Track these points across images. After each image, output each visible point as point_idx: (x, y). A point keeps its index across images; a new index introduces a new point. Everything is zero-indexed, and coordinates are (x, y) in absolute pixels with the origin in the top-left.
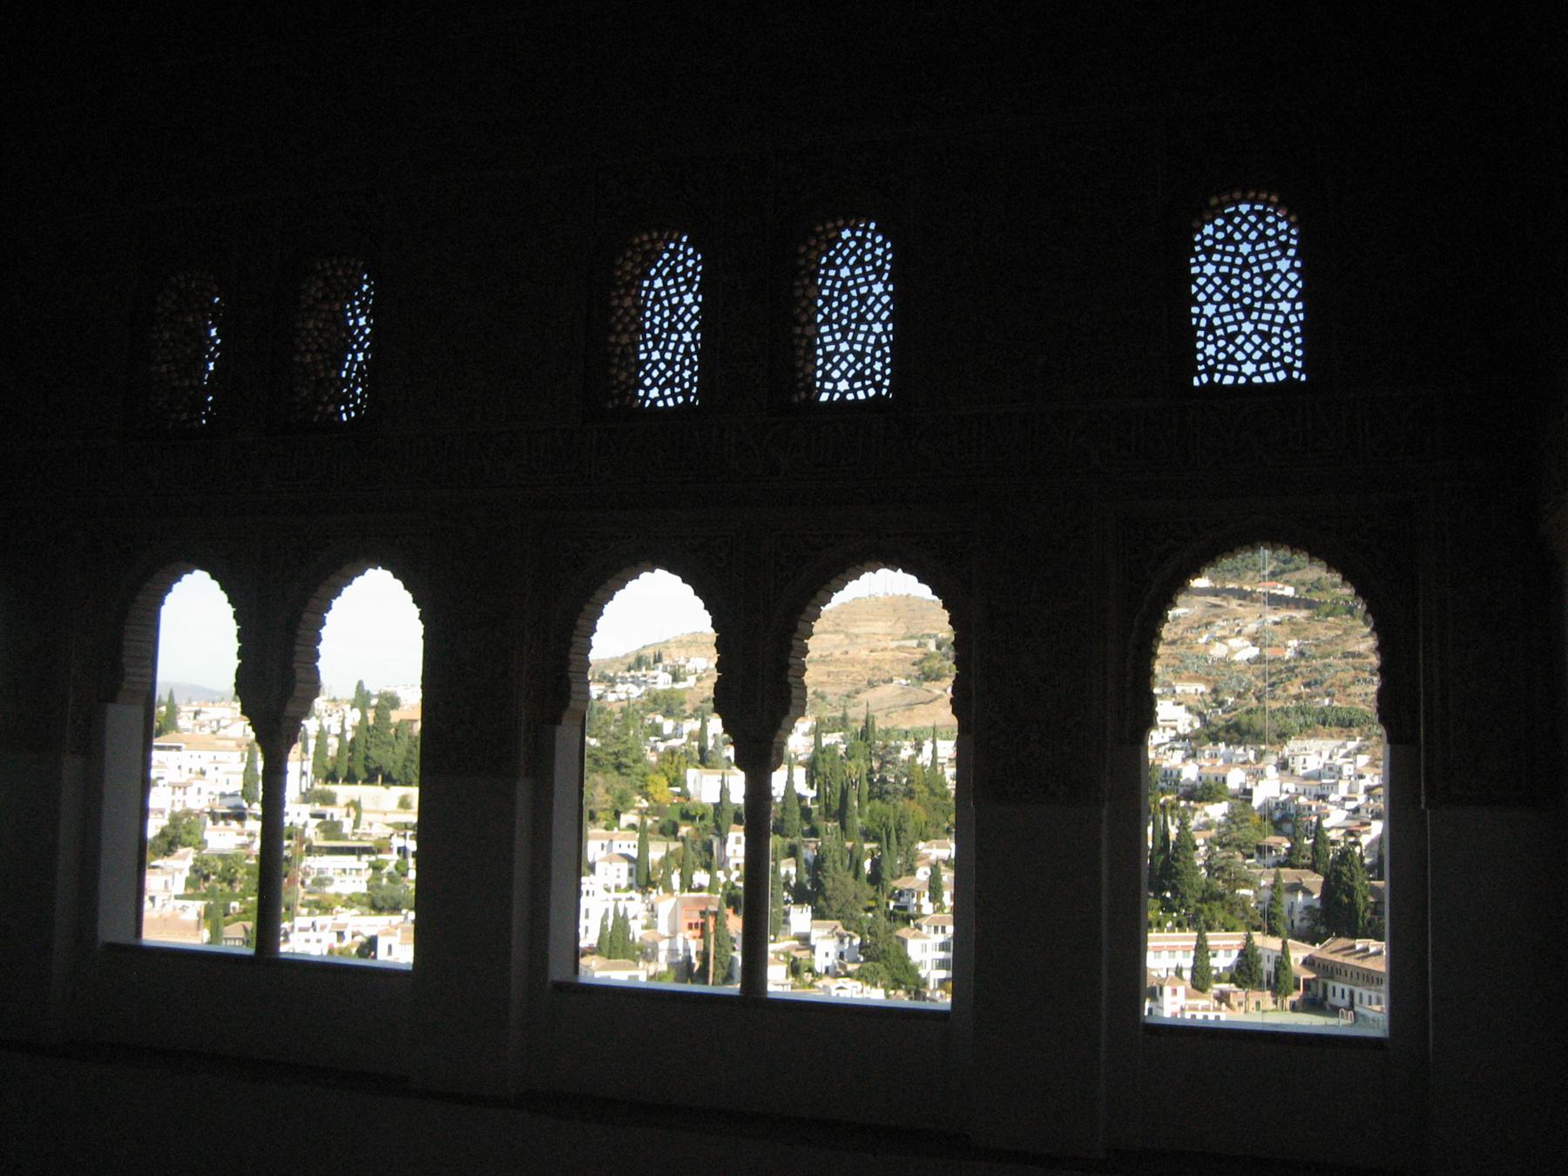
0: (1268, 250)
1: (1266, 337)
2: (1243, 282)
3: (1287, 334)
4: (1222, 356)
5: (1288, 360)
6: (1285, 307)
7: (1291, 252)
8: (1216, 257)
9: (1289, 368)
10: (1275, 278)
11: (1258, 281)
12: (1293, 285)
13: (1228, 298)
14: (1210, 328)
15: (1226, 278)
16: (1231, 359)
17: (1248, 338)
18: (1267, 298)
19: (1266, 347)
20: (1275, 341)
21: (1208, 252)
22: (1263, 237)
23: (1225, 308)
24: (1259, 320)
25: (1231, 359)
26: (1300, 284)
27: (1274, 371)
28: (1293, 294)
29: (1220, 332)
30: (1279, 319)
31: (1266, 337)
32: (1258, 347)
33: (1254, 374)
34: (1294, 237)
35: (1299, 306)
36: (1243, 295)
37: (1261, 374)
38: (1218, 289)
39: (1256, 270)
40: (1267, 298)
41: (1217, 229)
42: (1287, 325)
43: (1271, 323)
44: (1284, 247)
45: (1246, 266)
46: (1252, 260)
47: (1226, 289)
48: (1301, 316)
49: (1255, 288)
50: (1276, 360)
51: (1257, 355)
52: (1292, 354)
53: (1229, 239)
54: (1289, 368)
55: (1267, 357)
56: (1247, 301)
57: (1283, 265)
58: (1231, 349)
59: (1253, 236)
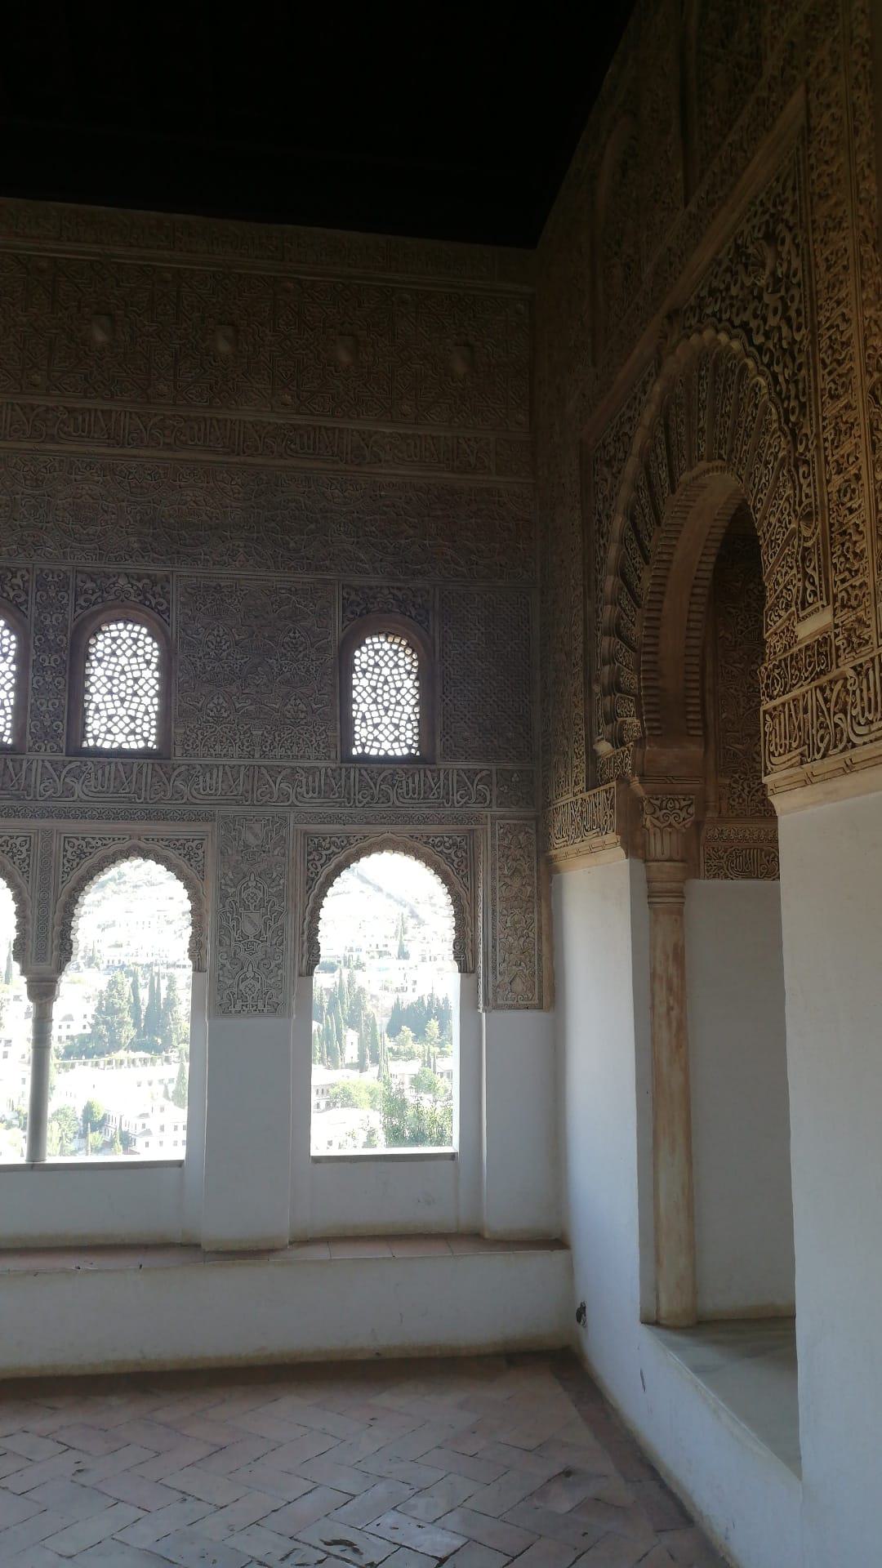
0: (138, 664)
1: (133, 719)
2: (121, 682)
3: (146, 718)
4: (104, 729)
5: (146, 735)
6: (146, 701)
7: (153, 666)
8: (104, 665)
9: (146, 740)
10: (141, 682)
11: (130, 683)
12: (153, 687)
13: (110, 692)
14: (97, 710)
15: (110, 679)
16: (109, 731)
17: (121, 718)
18: (135, 694)
19: (132, 726)
20: (139, 722)
21: (100, 660)
22: (135, 655)
23: (108, 698)
24: (129, 708)
25: (109, 731)
26: (157, 687)
27: (137, 741)
28: (152, 693)
29: (103, 713)
30: (142, 708)
31: (133, 719)
32: (127, 725)
33: (123, 742)
34: (155, 657)
35: (156, 701)
36: (120, 691)
37: (129, 742)
38: (104, 685)
39: (129, 675)
40: (135, 694)
41: (106, 646)
42: (147, 713)
43: (137, 711)
44: (148, 662)
45: (123, 672)
46: (127, 668)
47: (109, 685)
48: (156, 708)
49: (128, 687)
50: (138, 734)
51: (127, 730)
52: (149, 731)
53: (113, 654)
54: (146, 740)
55: (133, 732)
56: (122, 695)
57: (147, 674)
58: (110, 724)
59: (129, 653)
